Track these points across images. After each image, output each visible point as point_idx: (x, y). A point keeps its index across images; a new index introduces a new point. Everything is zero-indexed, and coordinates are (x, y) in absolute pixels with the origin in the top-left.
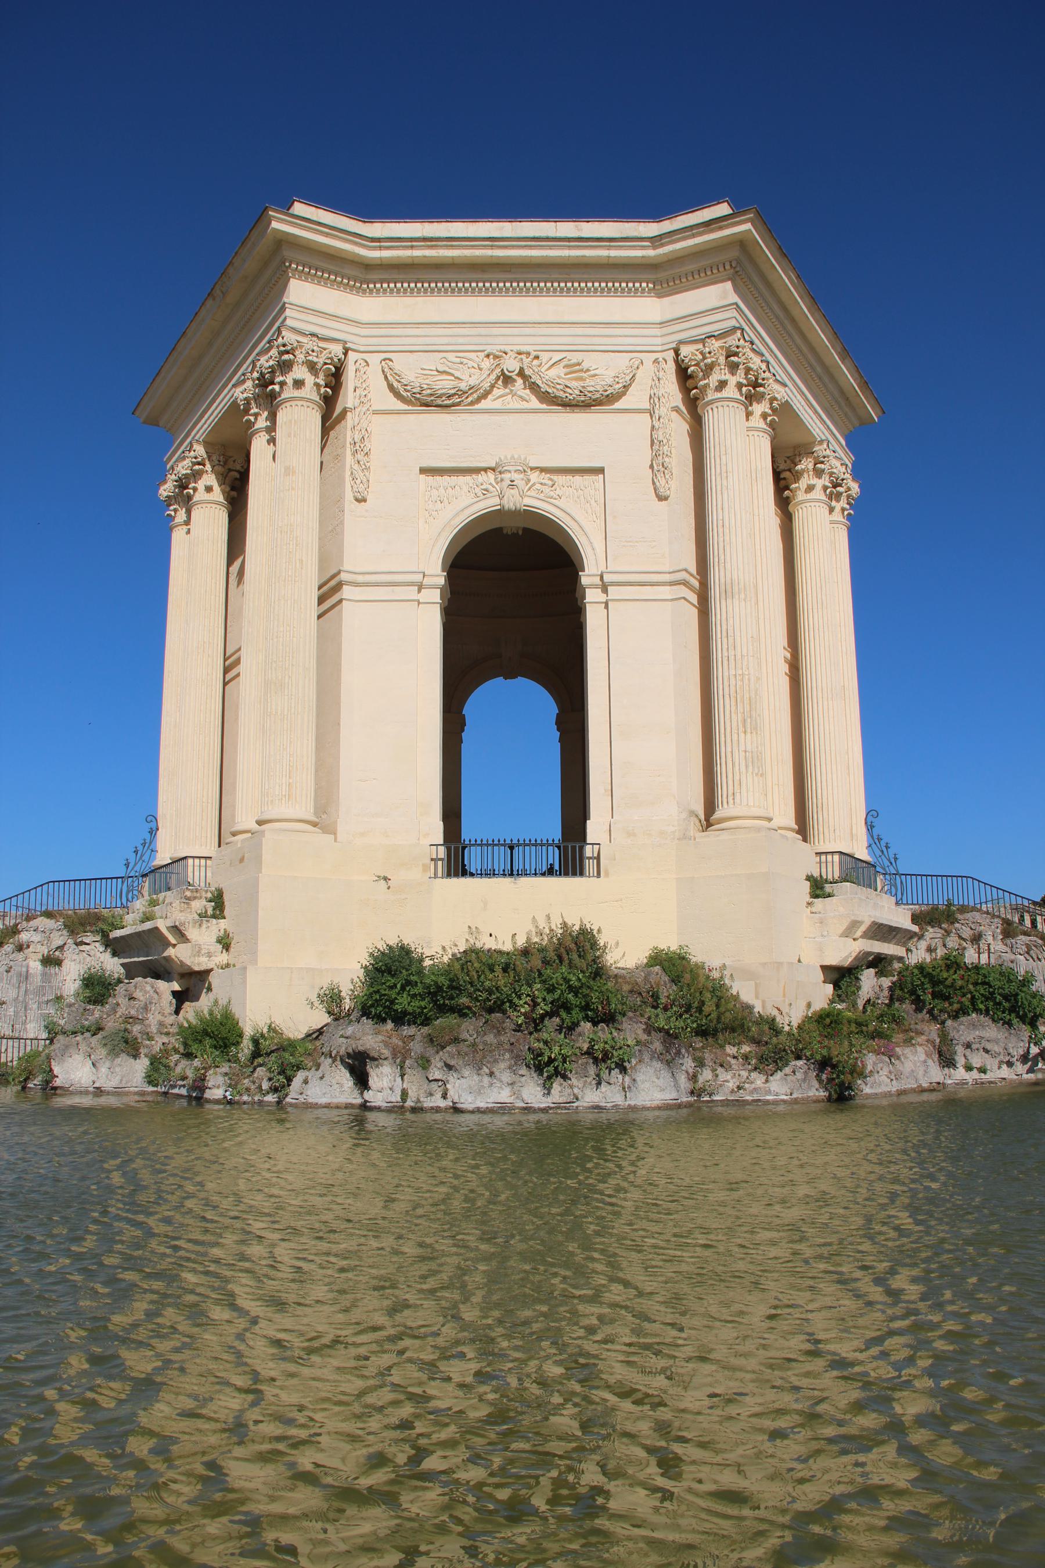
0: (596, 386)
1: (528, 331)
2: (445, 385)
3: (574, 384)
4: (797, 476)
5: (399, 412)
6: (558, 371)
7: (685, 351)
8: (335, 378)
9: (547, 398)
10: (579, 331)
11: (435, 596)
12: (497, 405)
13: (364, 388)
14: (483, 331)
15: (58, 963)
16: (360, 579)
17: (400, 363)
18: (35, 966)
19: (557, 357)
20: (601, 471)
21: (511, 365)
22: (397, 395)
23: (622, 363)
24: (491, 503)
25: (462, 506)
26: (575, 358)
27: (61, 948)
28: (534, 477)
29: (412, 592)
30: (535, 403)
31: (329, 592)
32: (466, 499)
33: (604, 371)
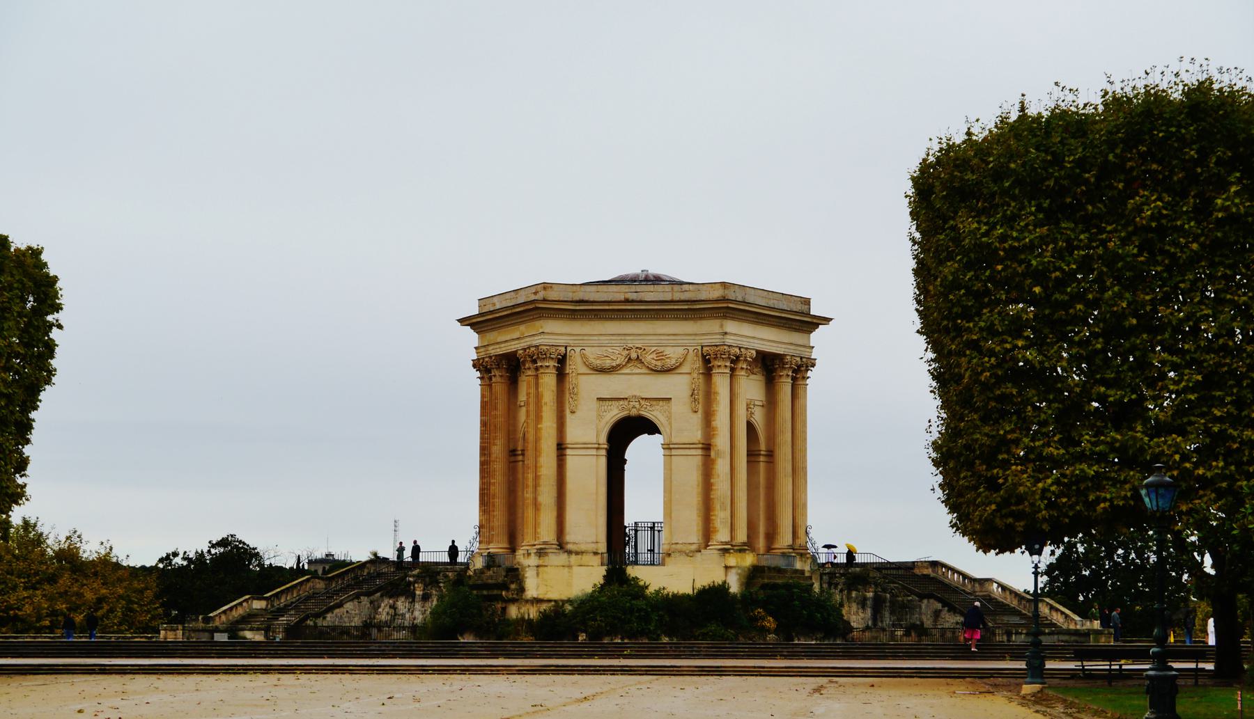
0: (670, 363)
2: (608, 363)
3: (659, 363)
4: (775, 370)
6: (654, 356)
8: (562, 360)
11: (604, 452)
13: (575, 366)
17: (588, 351)
21: (634, 356)
23: (681, 351)
25: (614, 413)
26: (661, 349)
28: (643, 402)
29: (594, 452)
30: (644, 370)
31: (561, 448)
32: (615, 411)
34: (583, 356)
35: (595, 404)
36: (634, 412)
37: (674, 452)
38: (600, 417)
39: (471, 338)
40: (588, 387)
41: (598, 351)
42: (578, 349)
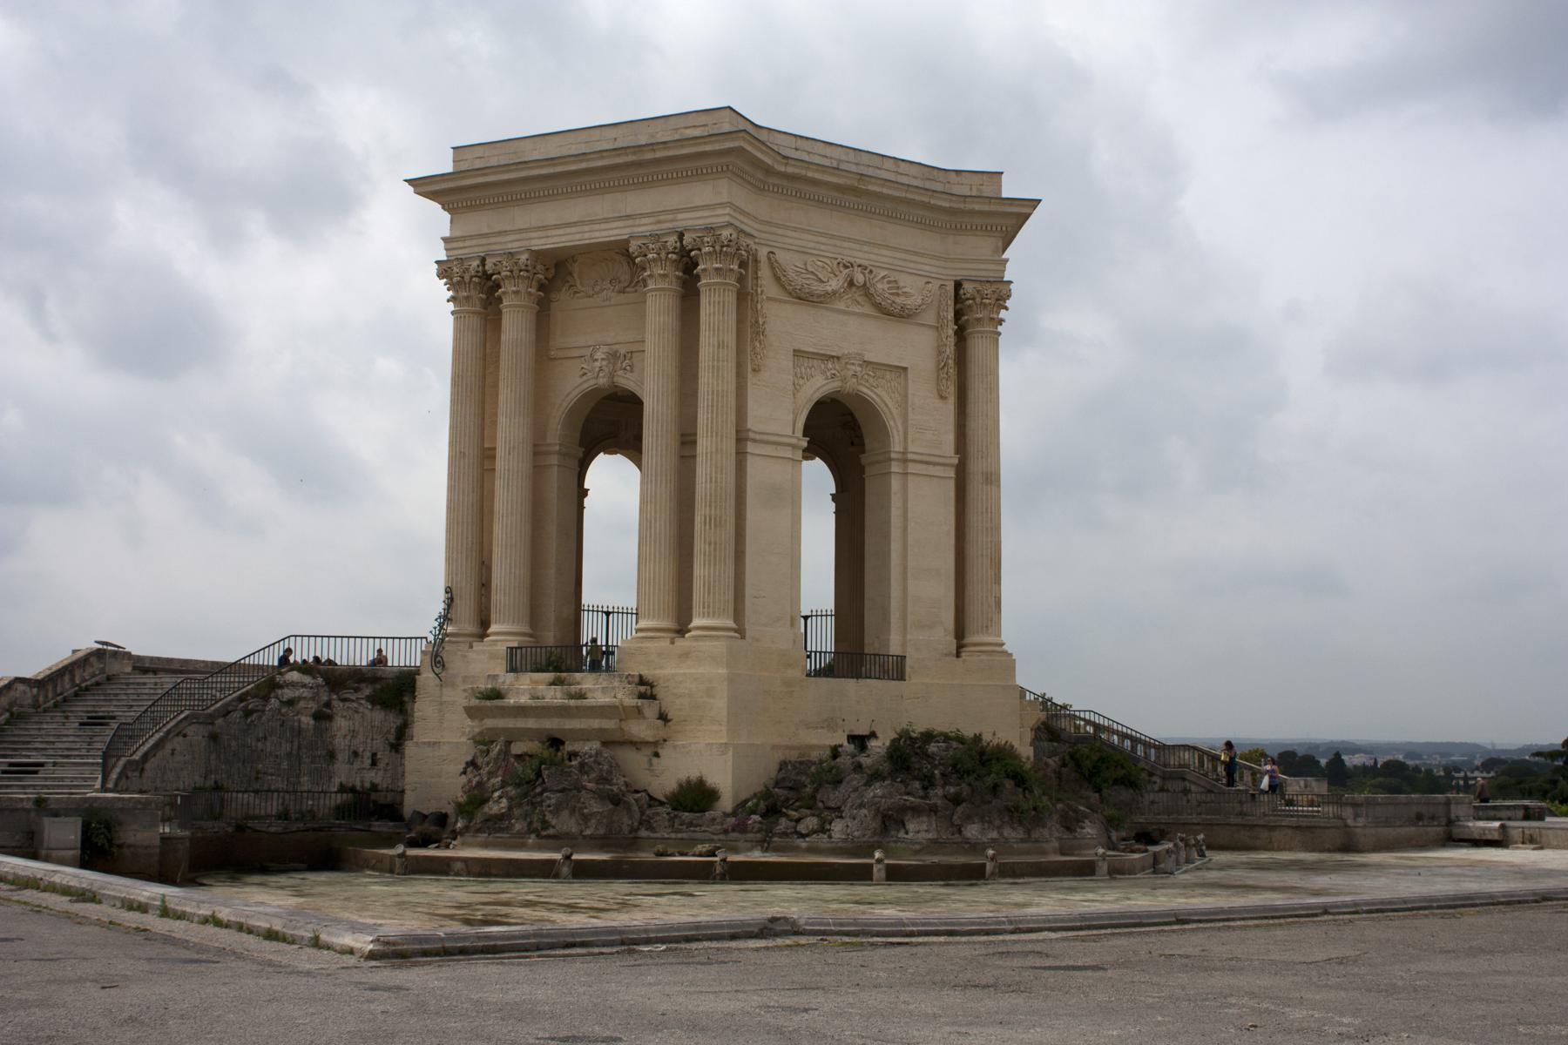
1: (866, 248)
5: (785, 302)
7: (968, 288)
9: (878, 307)
10: (898, 255)
12: (841, 306)
14: (838, 243)
15: (330, 718)
16: (758, 437)
18: (307, 721)
19: (883, 273)
20: (905, 369)
21: (859, 278)
22: (783, 287)
24: (834, 385)
26: (894, 276)
27: (328, 705)
30: (868, 309)
33: (914, 290)
34: (773, 264)
35: (787, 362)
36: (851, 385)
37: (912, 468)
38: (796, 388)
39: (437, 219)
40: (787, 326)
41: (798, 261)
42: (763, 253)
